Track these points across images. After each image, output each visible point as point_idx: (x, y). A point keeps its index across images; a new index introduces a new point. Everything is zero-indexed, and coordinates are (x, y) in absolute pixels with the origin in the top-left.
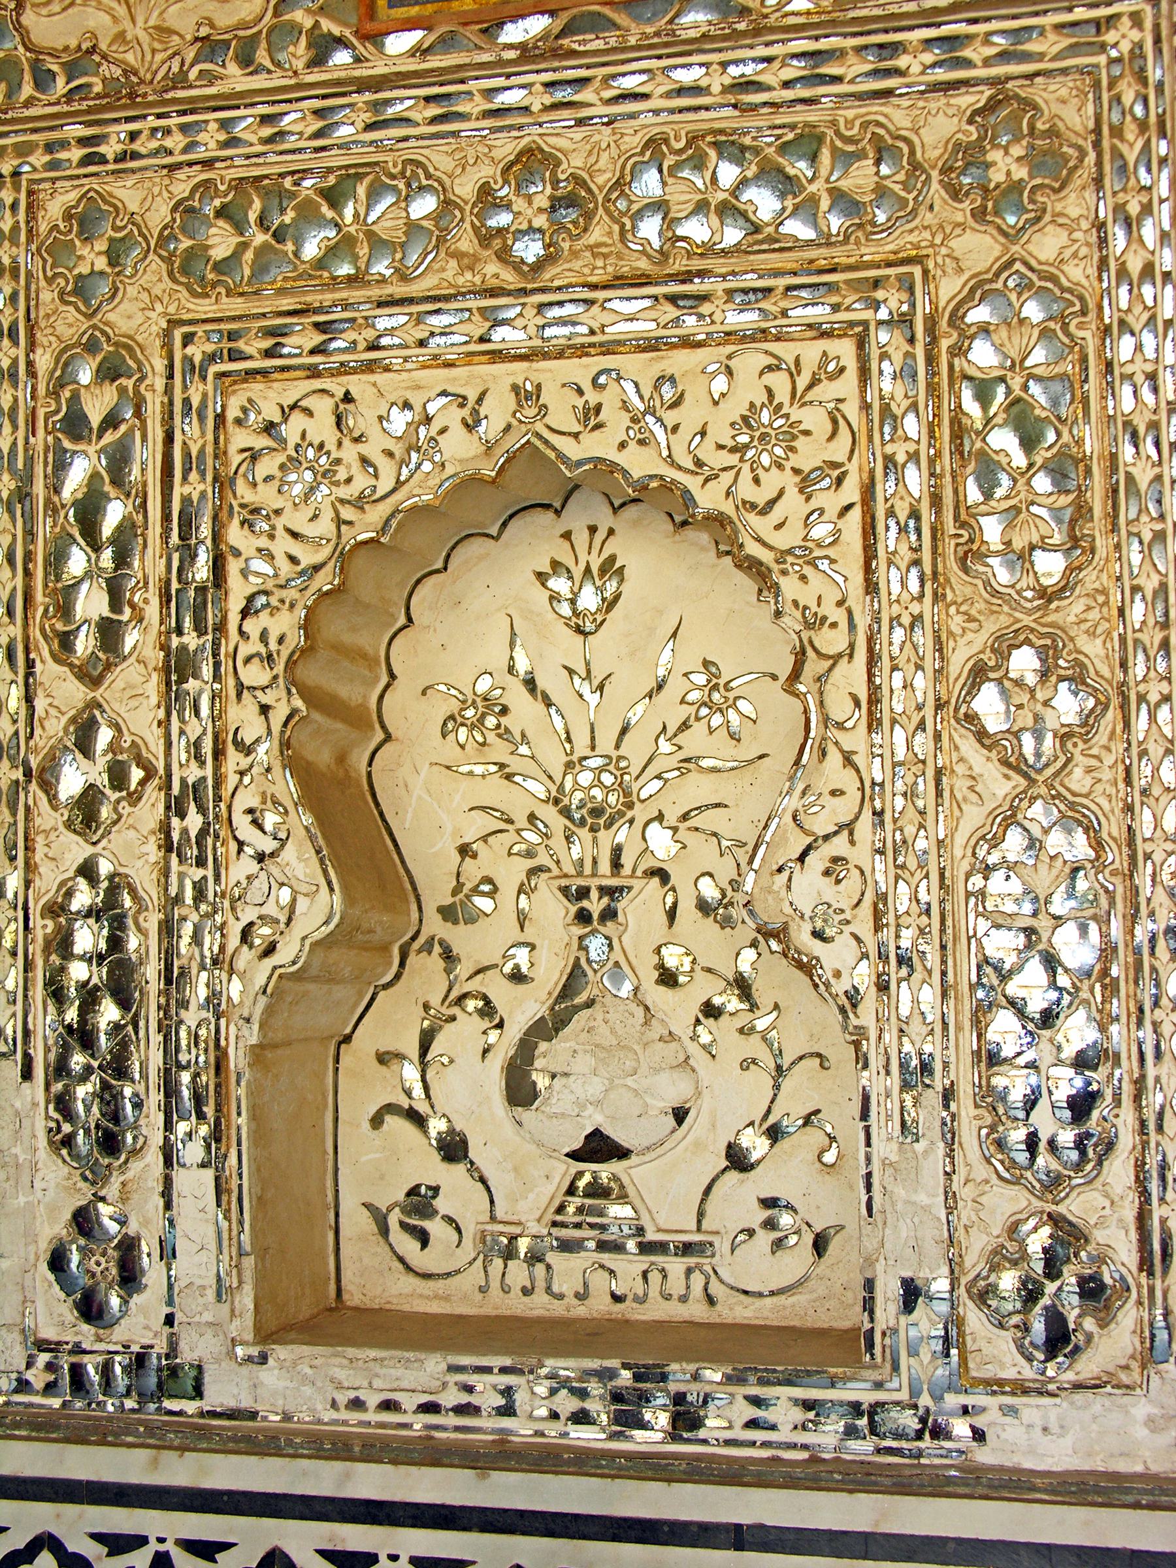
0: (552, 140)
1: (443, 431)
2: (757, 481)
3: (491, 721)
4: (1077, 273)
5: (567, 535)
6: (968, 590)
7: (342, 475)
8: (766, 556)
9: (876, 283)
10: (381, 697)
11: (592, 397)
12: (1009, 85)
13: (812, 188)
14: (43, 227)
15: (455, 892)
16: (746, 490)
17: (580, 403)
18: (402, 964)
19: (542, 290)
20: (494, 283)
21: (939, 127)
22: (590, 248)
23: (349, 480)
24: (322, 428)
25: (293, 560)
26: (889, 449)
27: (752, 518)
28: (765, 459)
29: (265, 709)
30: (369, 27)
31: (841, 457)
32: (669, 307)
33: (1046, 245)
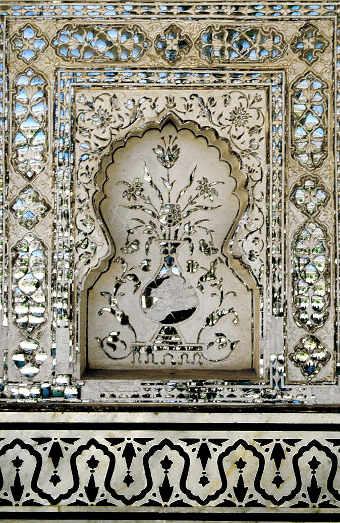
0: (179, 23)
1: (144, 109)
5: (163, 138)
6: (294, 164)
7: (112, 120)
8: (238, 152)
9: (272, 75)
11: (190, 102)
12: (311, 21)
14: (11, 34)
16: (233, 132)
17: (186, 103)
18: (109, 266)
19: (176, 69)
20: (161, 65)
21: (291, 31)
23: (114, 122)
24: (106, 105)
25: (97, 145)
26: (274, 123)
29: (87, 190)
31: (260, 124)
32: (214, 77)
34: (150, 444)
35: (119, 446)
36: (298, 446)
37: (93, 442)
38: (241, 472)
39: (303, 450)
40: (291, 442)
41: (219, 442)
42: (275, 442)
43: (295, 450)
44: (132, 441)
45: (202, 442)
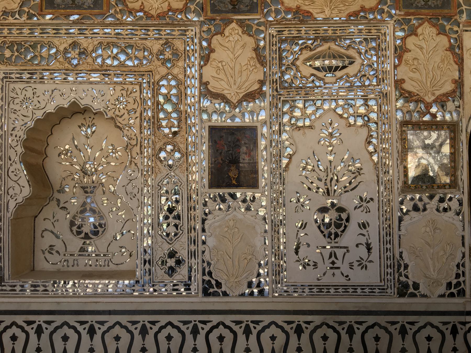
0: (79, 40)
2: (119, 111)
3: (69, 154)
4: (181, 77)
5: (85, 119)
8: (121, 126)
9: (143, 75)
10: (45, 149)
12: (169, 40)
13: (131, 55)
15: (60, 187)
16: (117, 113)
19: (77, 70)
20: (66, 68)
21: (156, 47)
22: (87, 63)
26: (145, 107)
27: (118, 118)
28: (121, 107)
30: (41, 13)
31: (136, 108)
32: (102, 76)
33: (175, 71)
34: (54, 325)
35: (32, 326)
36: (158, 325)
37: (14, 323)
38: (117, 344)
39: (162, 328)
40: (153, 323)
41: (102, 323)
42: (142, 323)
43: (156, 328)
44: (41, 323)
45: (90, 323)
